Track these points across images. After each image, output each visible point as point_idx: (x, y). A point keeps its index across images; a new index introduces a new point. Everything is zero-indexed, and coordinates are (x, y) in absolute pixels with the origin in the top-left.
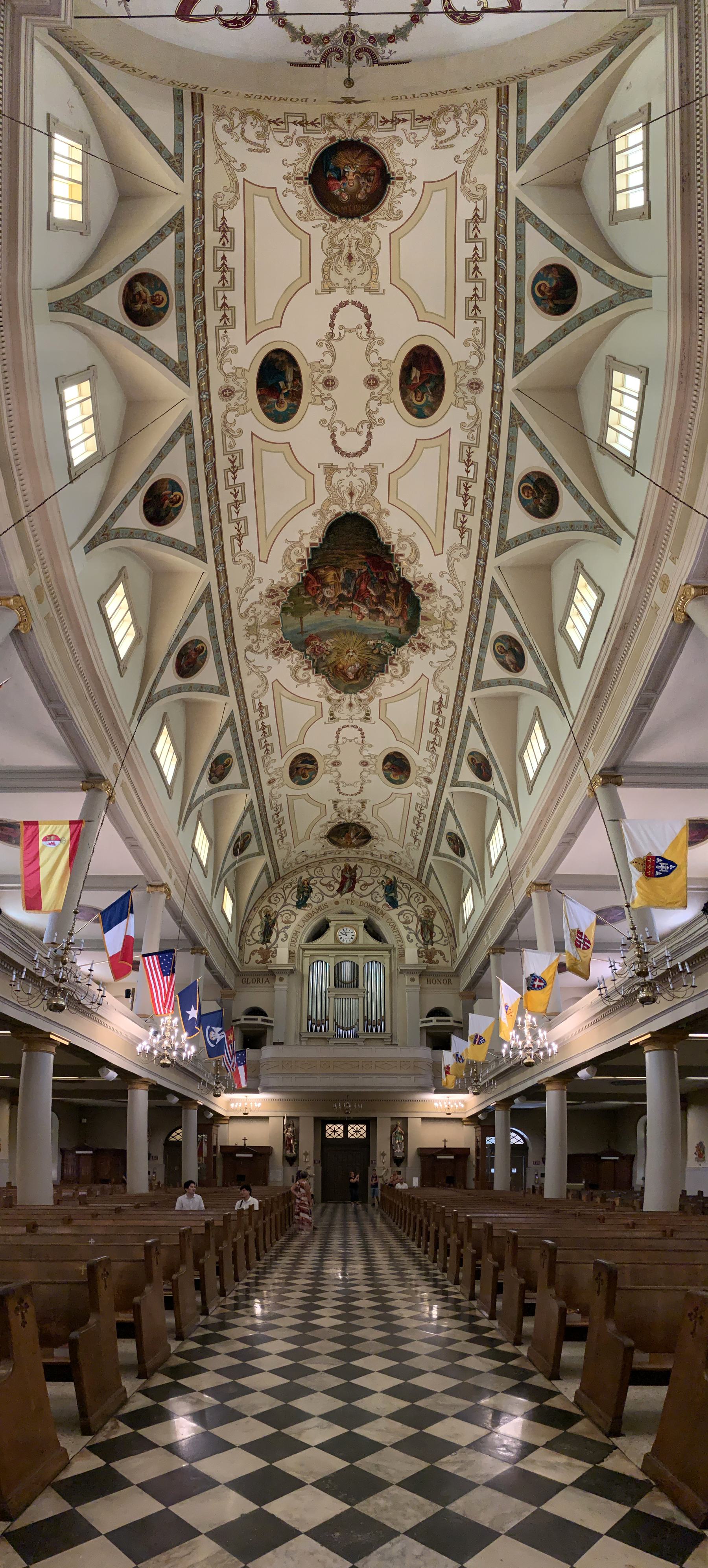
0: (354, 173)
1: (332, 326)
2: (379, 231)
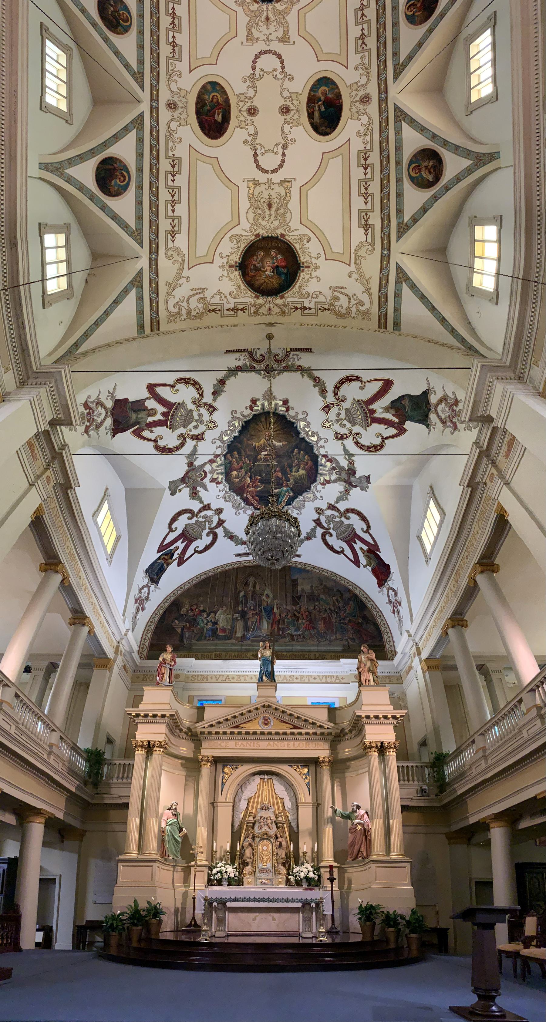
0: (266, 271)
1: (284, 155)
2: (247, 226)
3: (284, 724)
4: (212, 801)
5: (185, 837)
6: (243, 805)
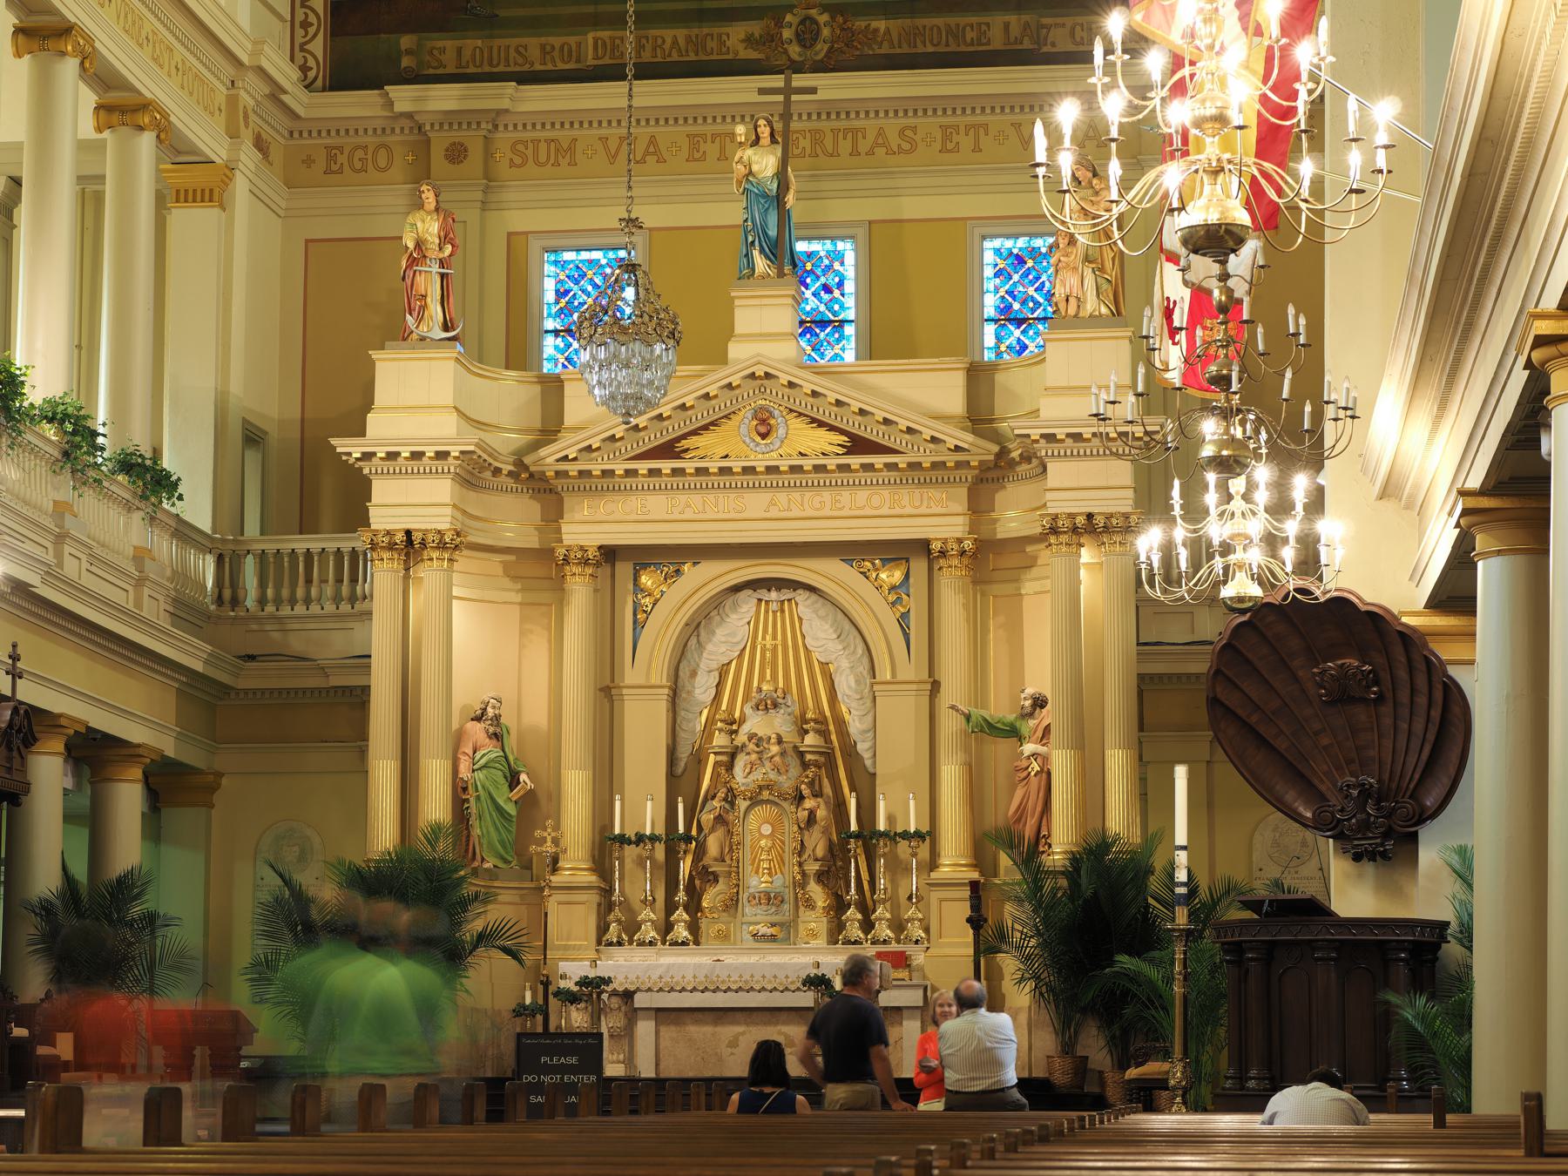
3: (822, 432)
4: (608, 682)
5: (529, 802)
6: (702, 690)
